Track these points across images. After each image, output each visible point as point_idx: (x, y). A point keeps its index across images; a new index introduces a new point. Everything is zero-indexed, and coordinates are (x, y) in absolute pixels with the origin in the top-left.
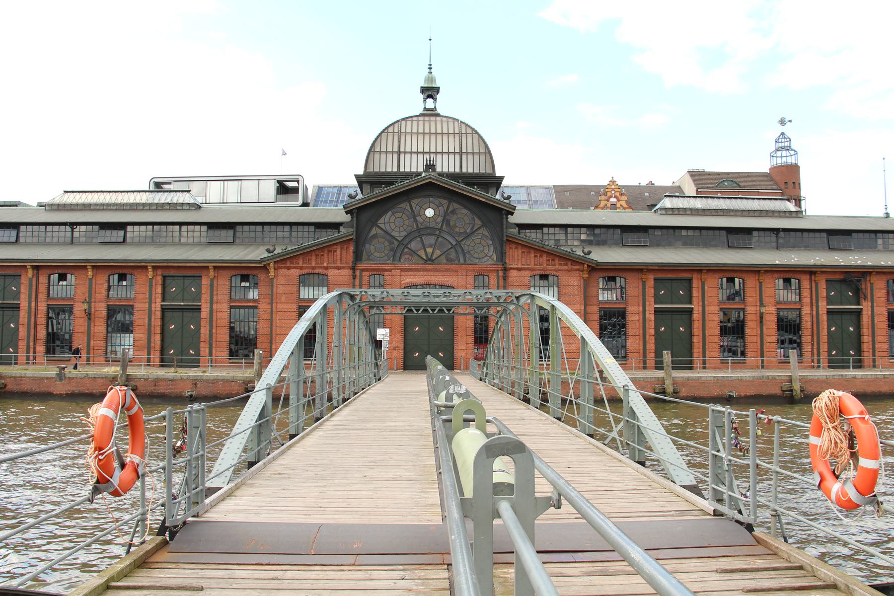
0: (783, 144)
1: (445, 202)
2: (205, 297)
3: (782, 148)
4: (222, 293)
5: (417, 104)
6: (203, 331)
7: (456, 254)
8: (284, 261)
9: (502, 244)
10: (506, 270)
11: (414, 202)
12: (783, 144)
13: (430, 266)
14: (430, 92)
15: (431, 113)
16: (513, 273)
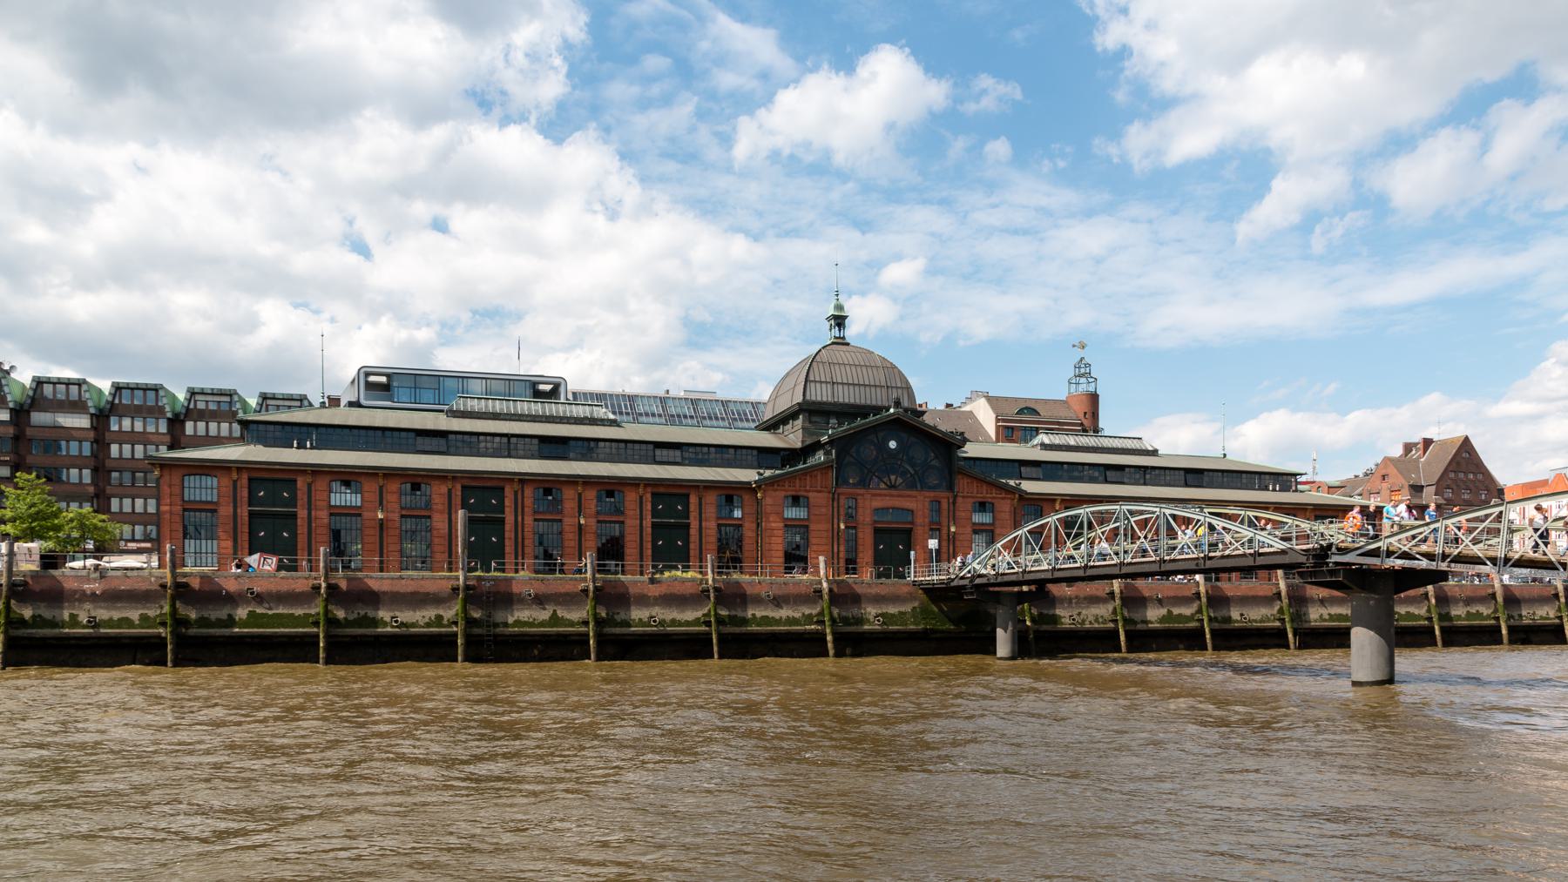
0: (1083, 371)
1: (904, 435)
2: (694, 514)
3: (1080, 376)
4: (710, 511)
5: (827, 335)
6: (692, 546)
7: (916, 482)
8: (772, 484)
9: (951, 473)
10: (955, 497)
11: (881, 435)
12: (1083, 371)
13: (894, 492)
14: (839, 321)
15: (841, 342)
16: (960, 500)
